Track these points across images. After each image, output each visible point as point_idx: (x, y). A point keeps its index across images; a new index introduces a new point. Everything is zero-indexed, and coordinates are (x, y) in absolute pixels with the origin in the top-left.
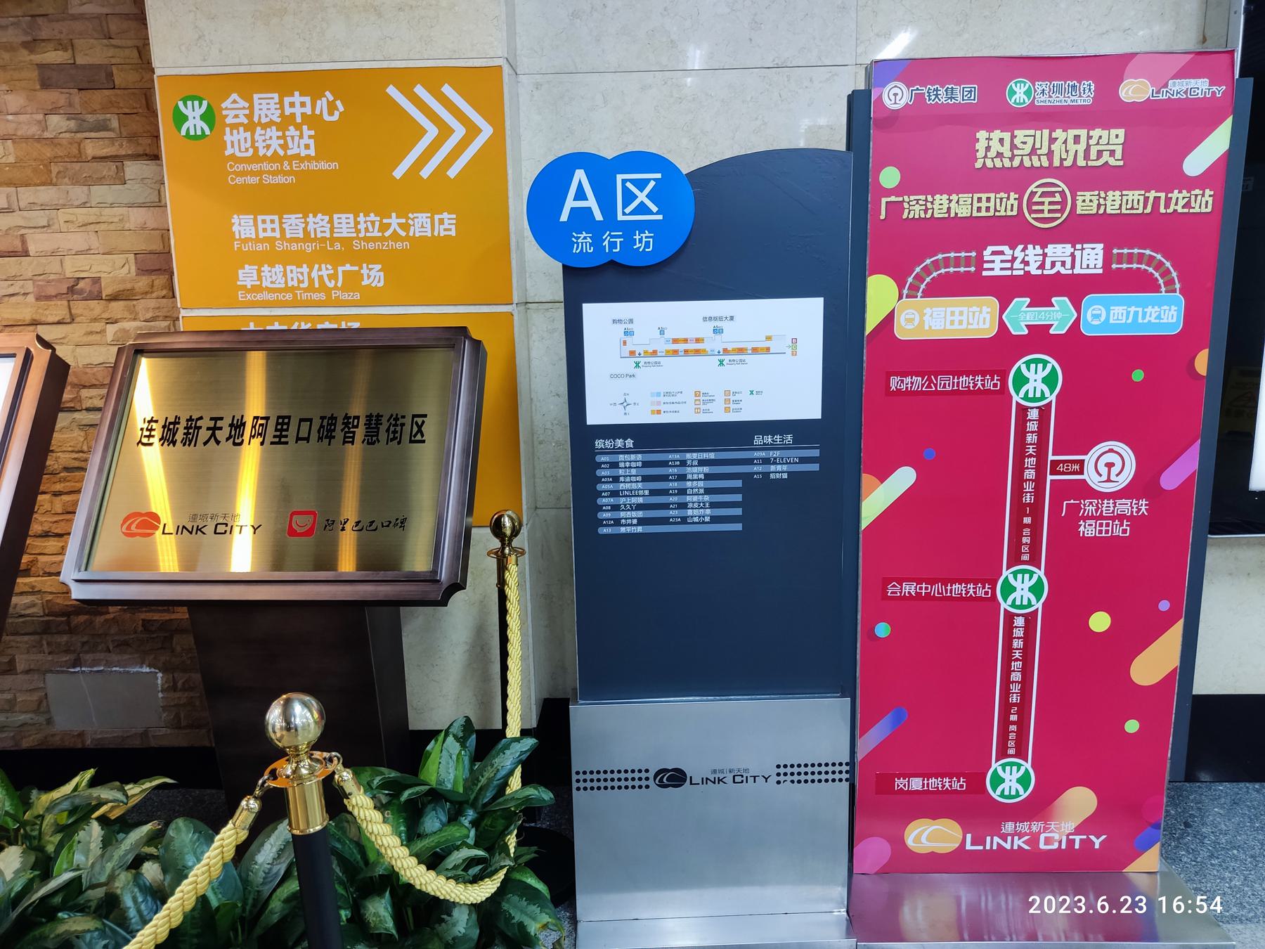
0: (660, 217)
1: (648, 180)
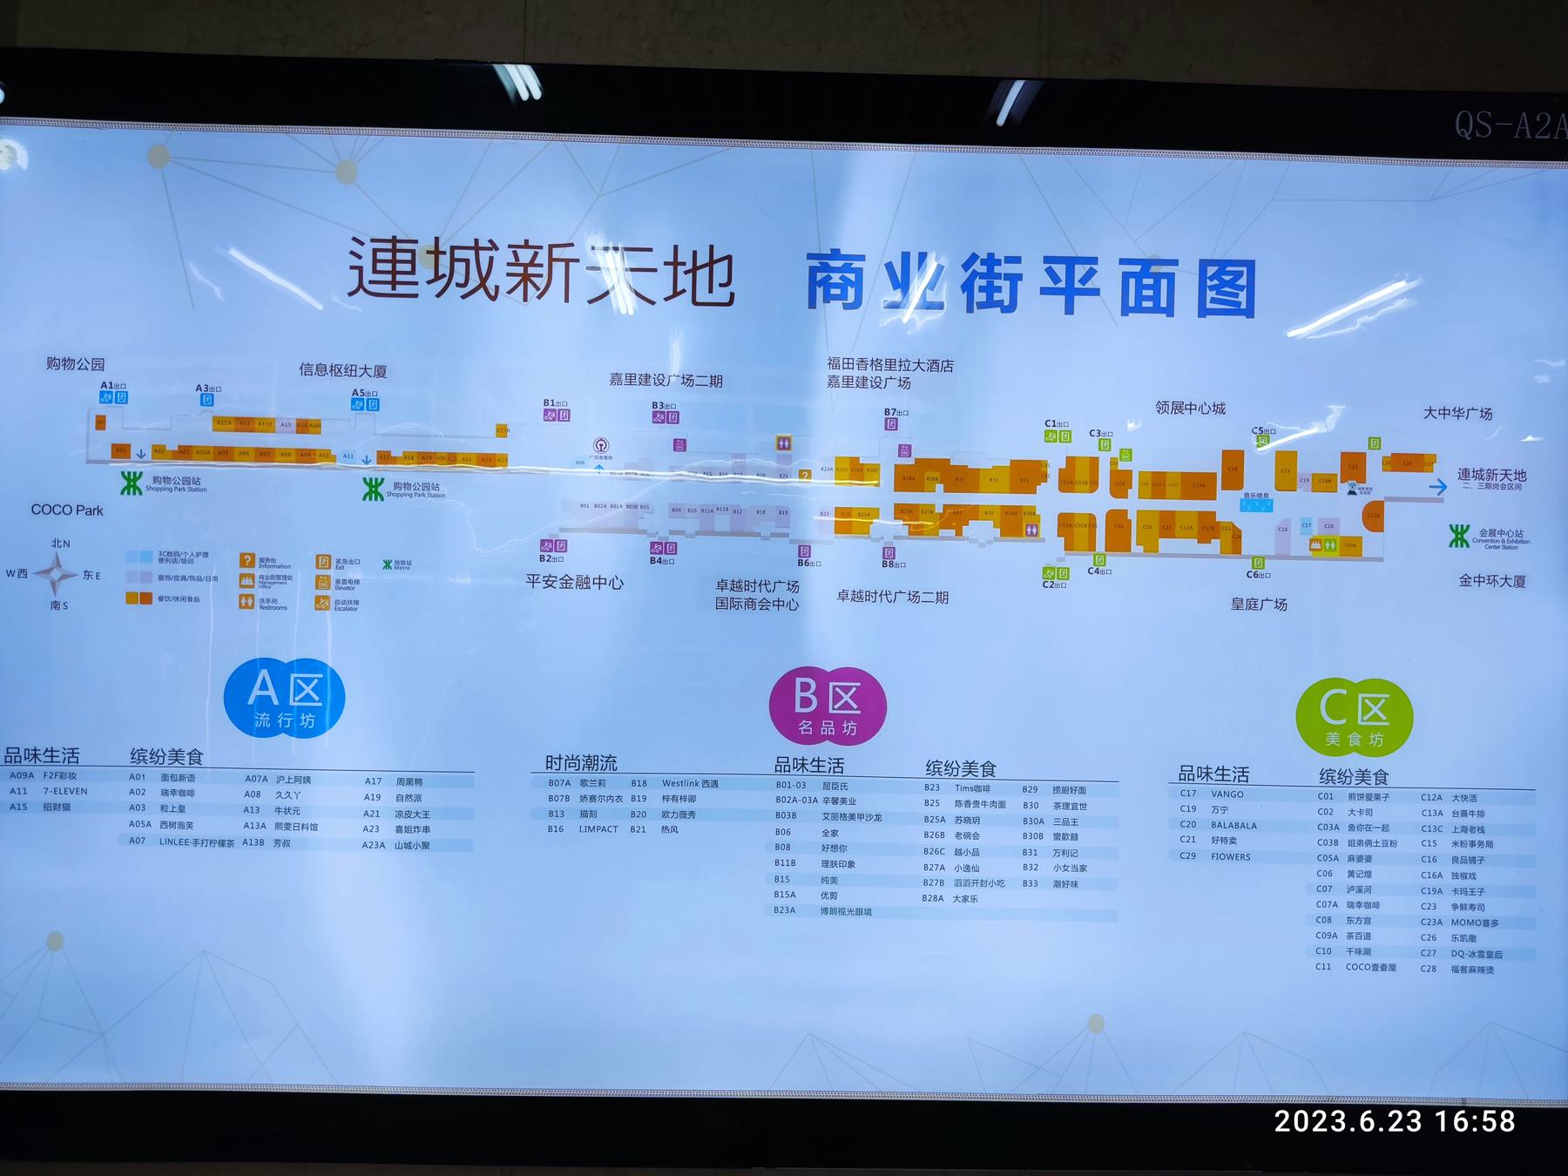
0: (859, 712)
1: (852, 687)
